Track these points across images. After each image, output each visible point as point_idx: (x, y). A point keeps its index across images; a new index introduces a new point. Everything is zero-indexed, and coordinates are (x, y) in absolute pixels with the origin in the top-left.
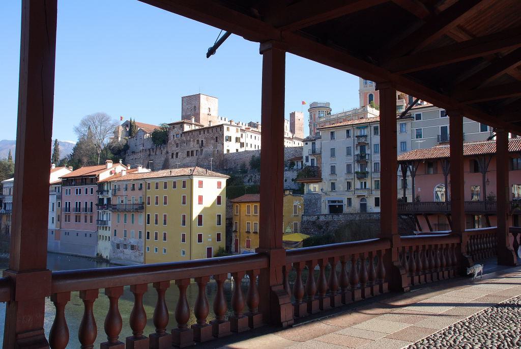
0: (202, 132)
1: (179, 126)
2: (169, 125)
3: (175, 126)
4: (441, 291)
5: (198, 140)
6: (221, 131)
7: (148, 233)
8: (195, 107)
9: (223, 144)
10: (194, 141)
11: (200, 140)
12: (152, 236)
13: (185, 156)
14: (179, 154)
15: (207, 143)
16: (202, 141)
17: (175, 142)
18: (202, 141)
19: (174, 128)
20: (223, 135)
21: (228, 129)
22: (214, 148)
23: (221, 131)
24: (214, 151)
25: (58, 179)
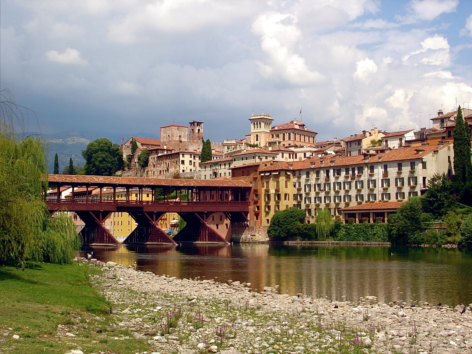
0: (168, 157)
1: (155, 151)
2: (149, 151)
3: (153, 152)
4: (288, 257)
5: (166, 163)
6: (178, 156)
7: (115, 222)
8: (169, 136)
9: (179, 166)
10: (164, 163)
11: (167, 163)
12: (116, 223)
13: (159, 174)
14: (155, 173)
15: (171, 165)
16: (168, 163)
17: (153, 163)
18: (168, 163)
19: (152, 153)
20: (179, 159)
21: (183, 155)
22: (175, 169)
23: (178, 156)
24: (175, 171)
25: (70, 194)
